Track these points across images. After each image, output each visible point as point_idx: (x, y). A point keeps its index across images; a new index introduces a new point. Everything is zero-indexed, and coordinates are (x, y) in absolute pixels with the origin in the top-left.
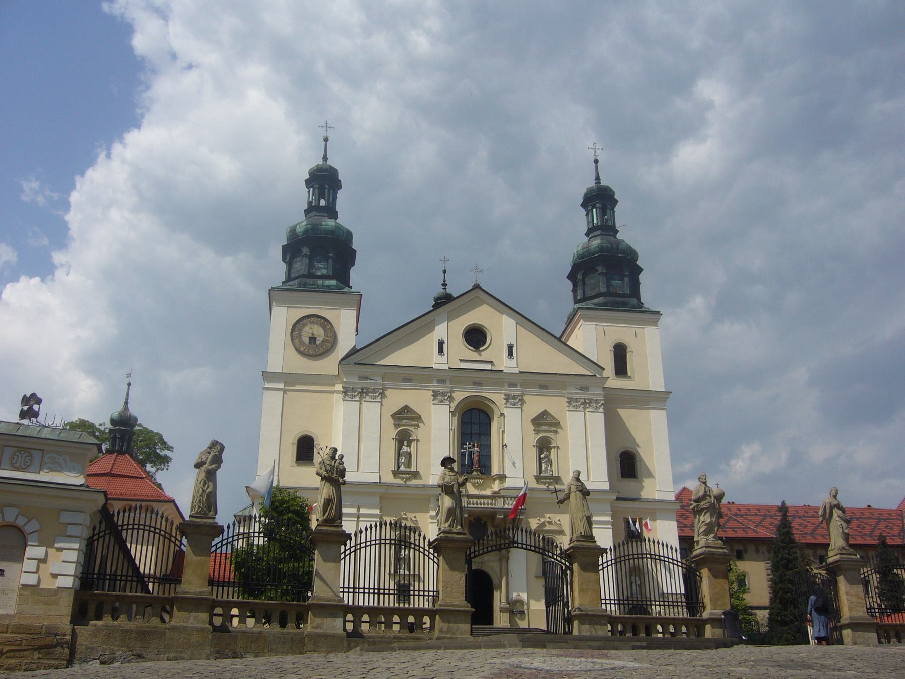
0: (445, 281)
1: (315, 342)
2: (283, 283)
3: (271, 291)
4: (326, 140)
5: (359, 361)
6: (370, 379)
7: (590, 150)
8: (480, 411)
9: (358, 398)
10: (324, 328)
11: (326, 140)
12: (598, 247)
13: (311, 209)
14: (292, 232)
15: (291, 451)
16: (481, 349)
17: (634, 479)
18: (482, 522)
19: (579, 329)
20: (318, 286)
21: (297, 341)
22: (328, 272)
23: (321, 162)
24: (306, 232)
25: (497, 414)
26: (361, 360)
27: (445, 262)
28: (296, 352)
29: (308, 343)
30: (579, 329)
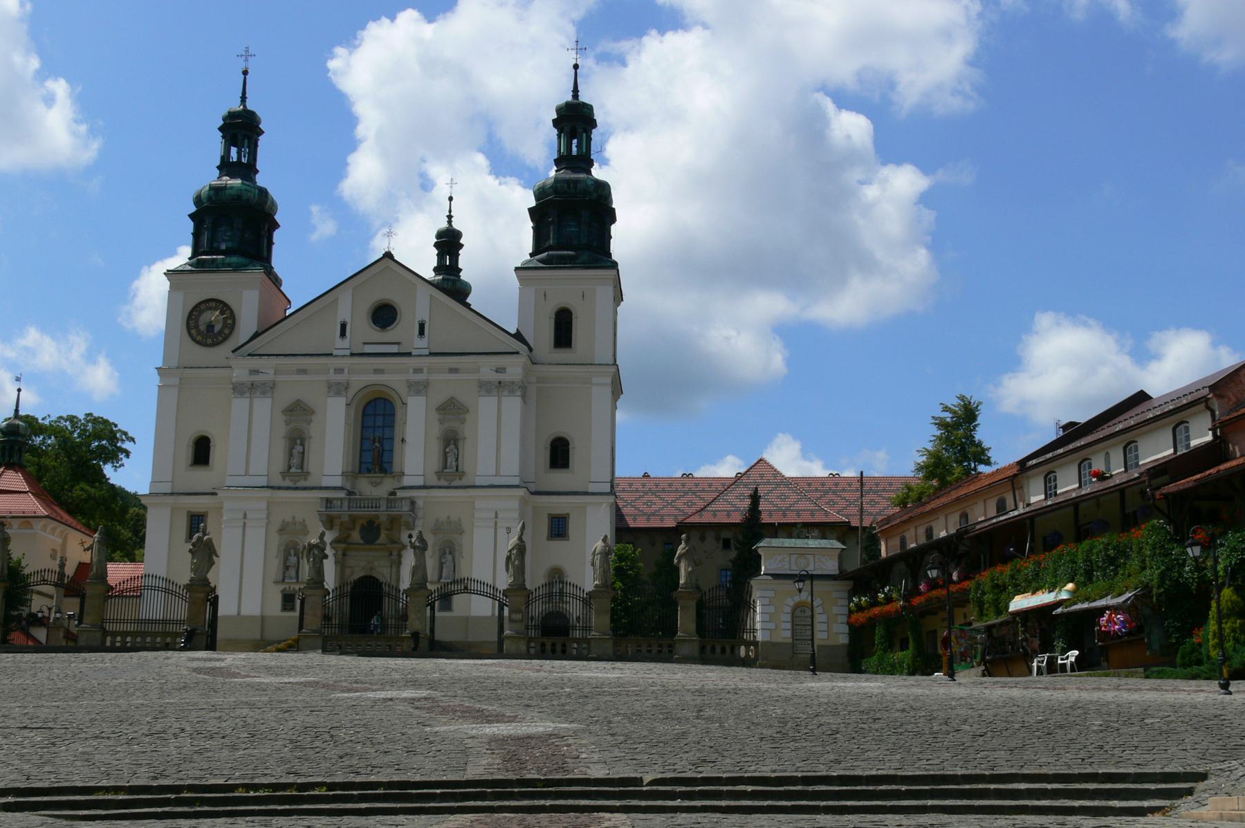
0: (450, 211)
1: (213, 332)
4: (245, 73)
7: (570, 50)
8: (385, 400)
9: (248, 395)
11: (245, 73)
12: (552, 187)
13: (226, 167)
15: (187, 453)
16: (388, 328)
17: (565, 470)
18: (375, 525)
21: (193, 332)
24: (209, 198)
25: (398, 404)
27: (451, 187)
28: (193, 343)
29: (205, 332)
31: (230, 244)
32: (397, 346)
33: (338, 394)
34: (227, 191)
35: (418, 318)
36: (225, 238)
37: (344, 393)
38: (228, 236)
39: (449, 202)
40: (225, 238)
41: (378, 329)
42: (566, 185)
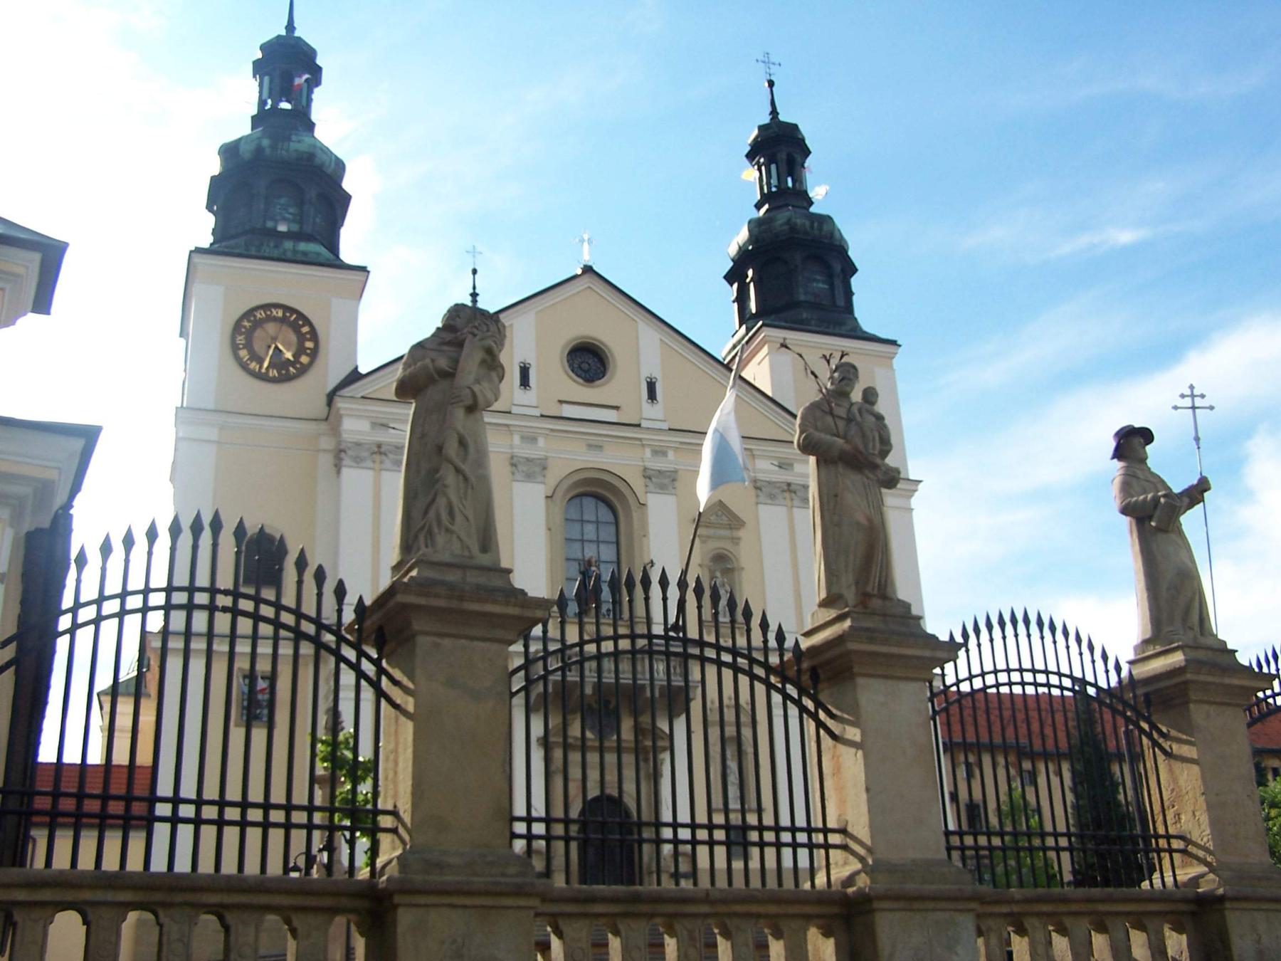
0: (474, 288)
2: (211, 244)
3: (193, 255)
5: (367, 394)
6: (394, 428)
10: (296, 329)
12: (788, 222)
14: (229, 152)
19: (759, 364)
20: (285, 251)
22: (301, 228)
23: (283, 33)
26: (370, 393)
27: (474, 256)
30: (759, 364)
31: (295, 227)
32: (614, 412)
33: (529, 477)
34: (292, 144)
35: (645, 373)
36: (287, 215)
37: (540, 479)
38: (290, 214)
39: (472, 276)
40: (287, 215)
41: (580, 380)
42: (808, 223)
